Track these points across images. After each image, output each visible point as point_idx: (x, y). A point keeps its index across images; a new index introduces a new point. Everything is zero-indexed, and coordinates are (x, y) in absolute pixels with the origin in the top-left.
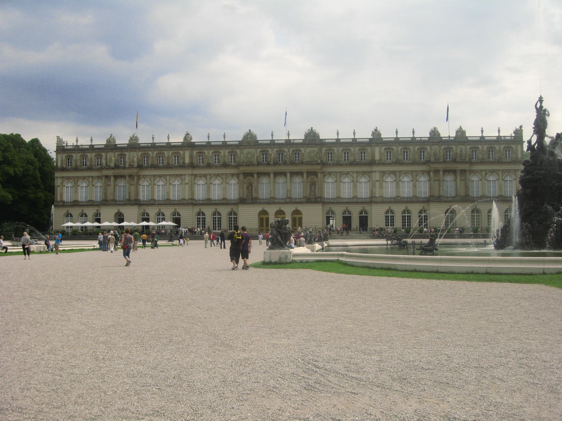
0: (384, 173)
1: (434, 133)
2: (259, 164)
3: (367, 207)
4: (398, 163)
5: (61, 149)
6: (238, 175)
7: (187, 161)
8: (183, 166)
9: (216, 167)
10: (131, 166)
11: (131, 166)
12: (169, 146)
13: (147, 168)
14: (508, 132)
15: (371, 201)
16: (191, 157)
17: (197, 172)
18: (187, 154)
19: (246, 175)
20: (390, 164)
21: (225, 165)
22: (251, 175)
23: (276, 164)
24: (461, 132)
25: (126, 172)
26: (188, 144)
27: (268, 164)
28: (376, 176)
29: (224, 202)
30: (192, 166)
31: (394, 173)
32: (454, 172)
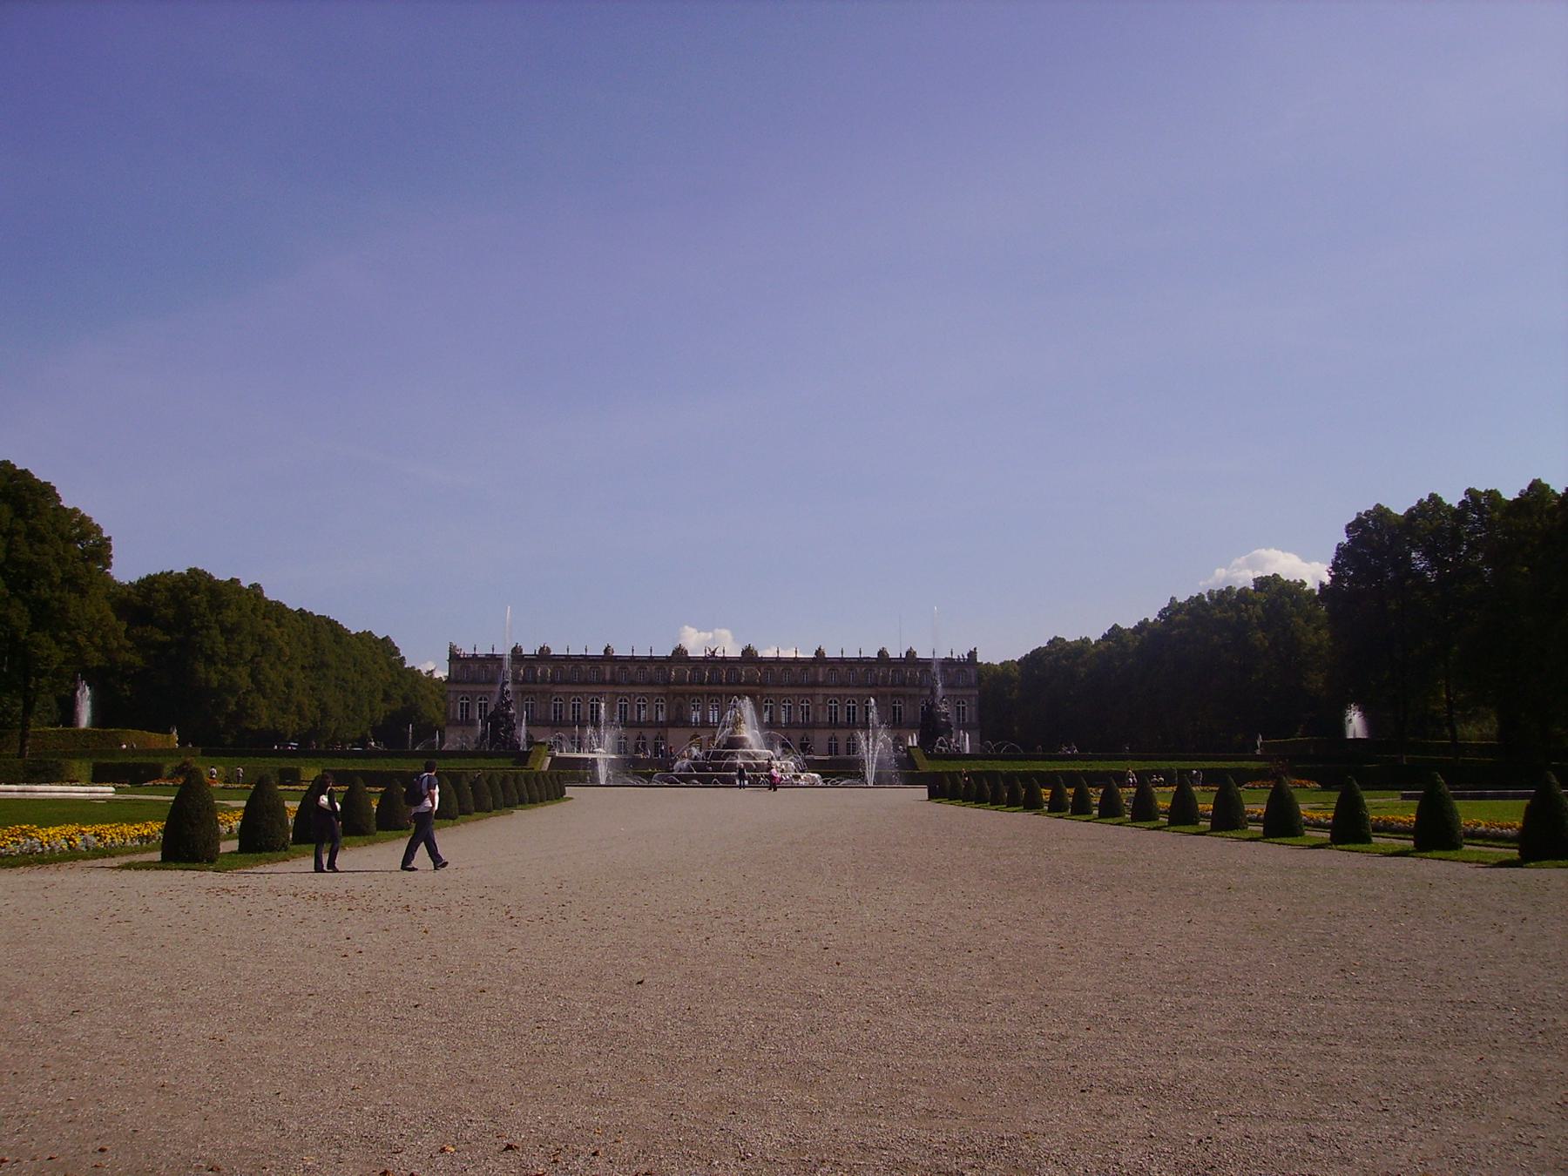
0: (827, 696)
1: (882, 653)
2: (691, 683)
3: (809, 733)
4: (842, 685)
5: (454, 657)
6: (666, 695)
7: (608, 677)
8: (604, 683)
9: (641, 684)
10: (544, 681)
11: (544, 681)
12: (585, 659)
13: (561, 683)
14: (961, 652)
15: (814, 726)
16: (612, 673)
17: (621, 690)
18: (608, 669)
19: (676, 695)
20: (835, 686)
21: (651, 683)
22: (682, 695)
23: (710, 683)
24: (910, 653)
25: (538, 687)
26: (608, 657)
27: (702, 683)
28: (820, 700)
29: (653, 724)
30: (613, 682)
31: (839, 696)
32: (903, 696)
